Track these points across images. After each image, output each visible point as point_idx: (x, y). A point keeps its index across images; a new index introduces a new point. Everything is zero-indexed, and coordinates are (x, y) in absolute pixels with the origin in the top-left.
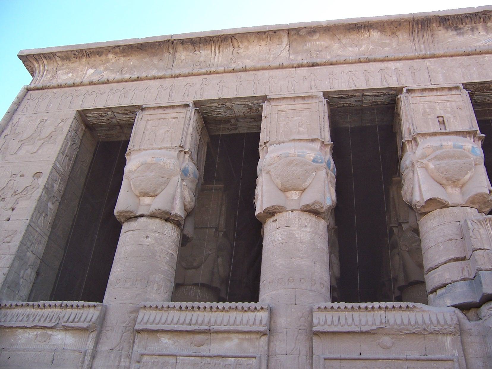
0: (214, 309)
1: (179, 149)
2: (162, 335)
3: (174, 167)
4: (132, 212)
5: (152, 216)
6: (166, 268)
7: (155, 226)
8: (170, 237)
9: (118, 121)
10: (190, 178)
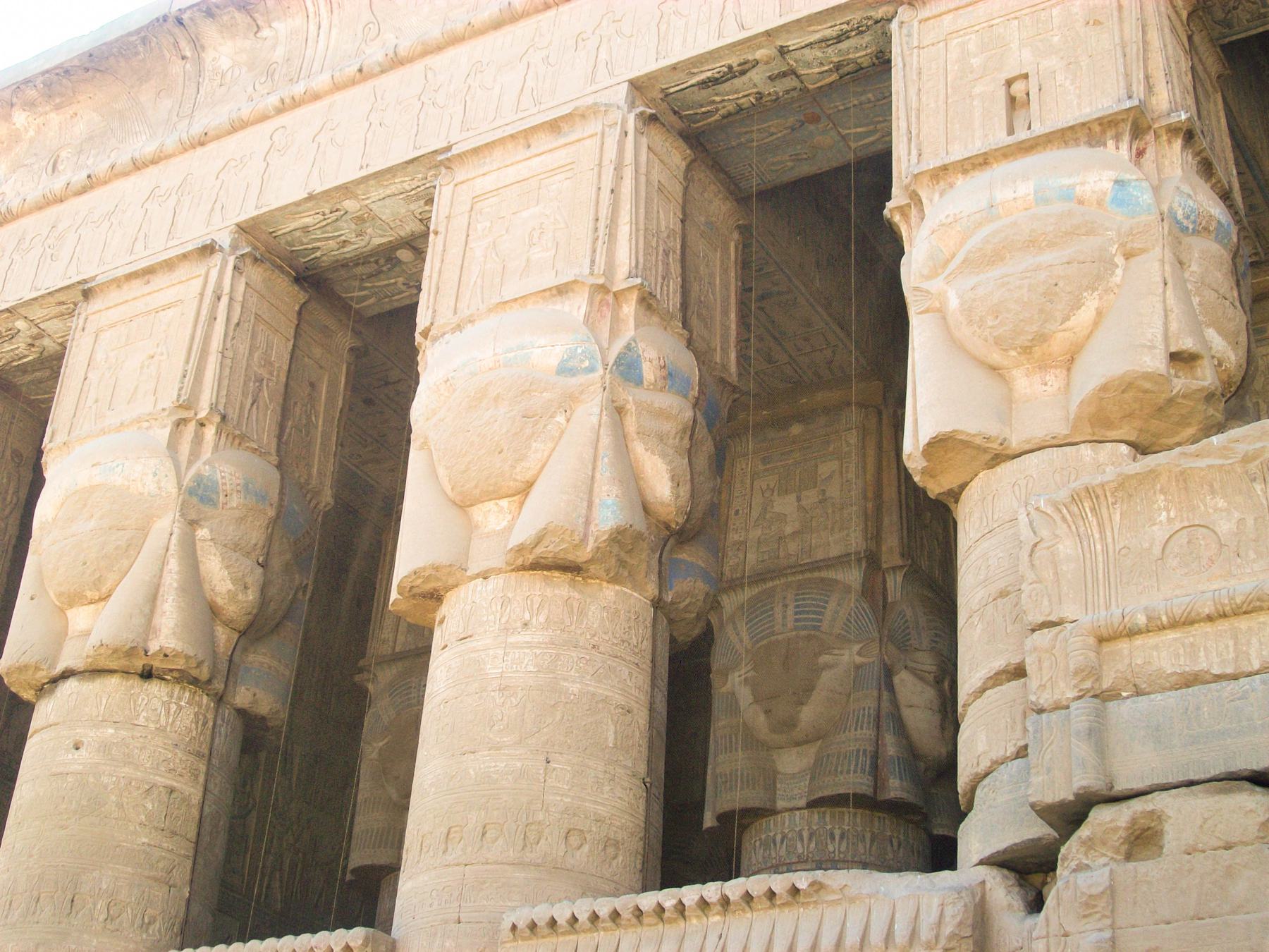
1: (175, 418)
3: (159, 482)
5: (96, 672)
6: (145, 840)
7: (104, 701)
8: (161, 730)
10: (233, 508)
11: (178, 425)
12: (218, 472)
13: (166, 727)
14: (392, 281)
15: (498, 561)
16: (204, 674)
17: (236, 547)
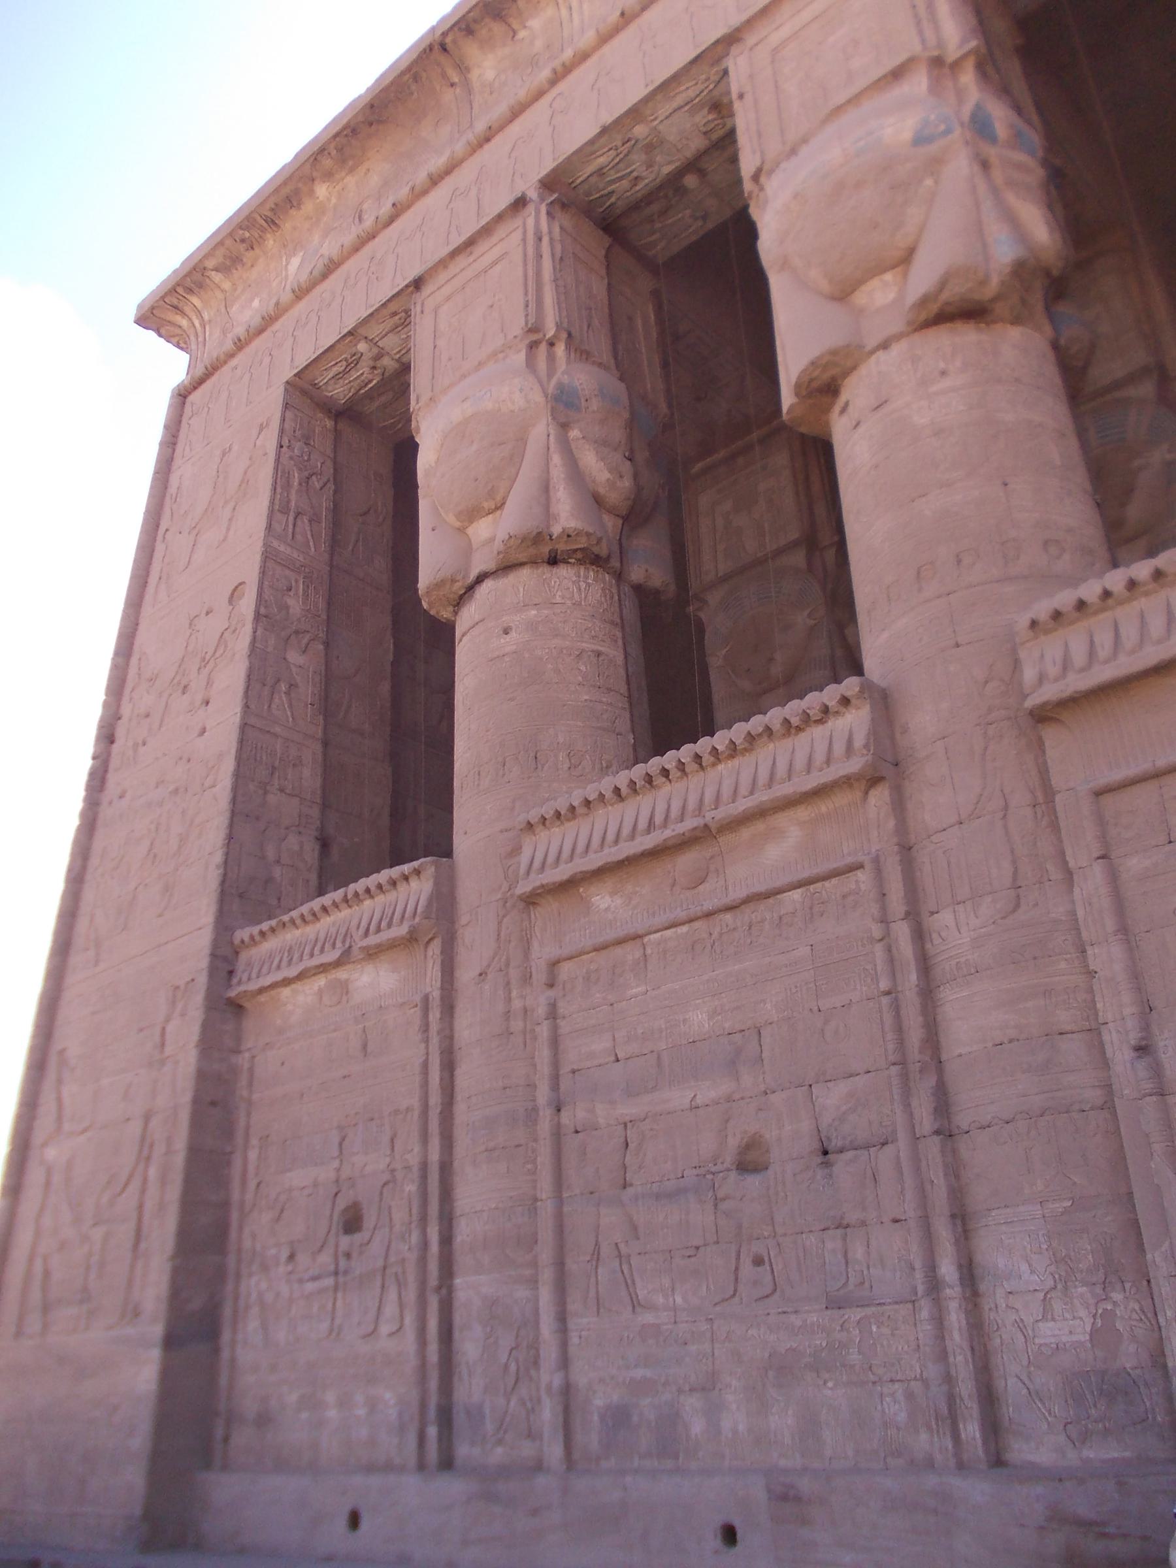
0: (707, 759)
1: (527, 342)
2: (593, 889)
4: (453, 581)
5: (506, 568)
7: (521, 590)
9: (398, 361)
10: (594, 412)
11: (531, 348)
12: (576, 381)
13: (581, 602)
14: (680, 215)
15: (897, 325)
16: (604, 553)
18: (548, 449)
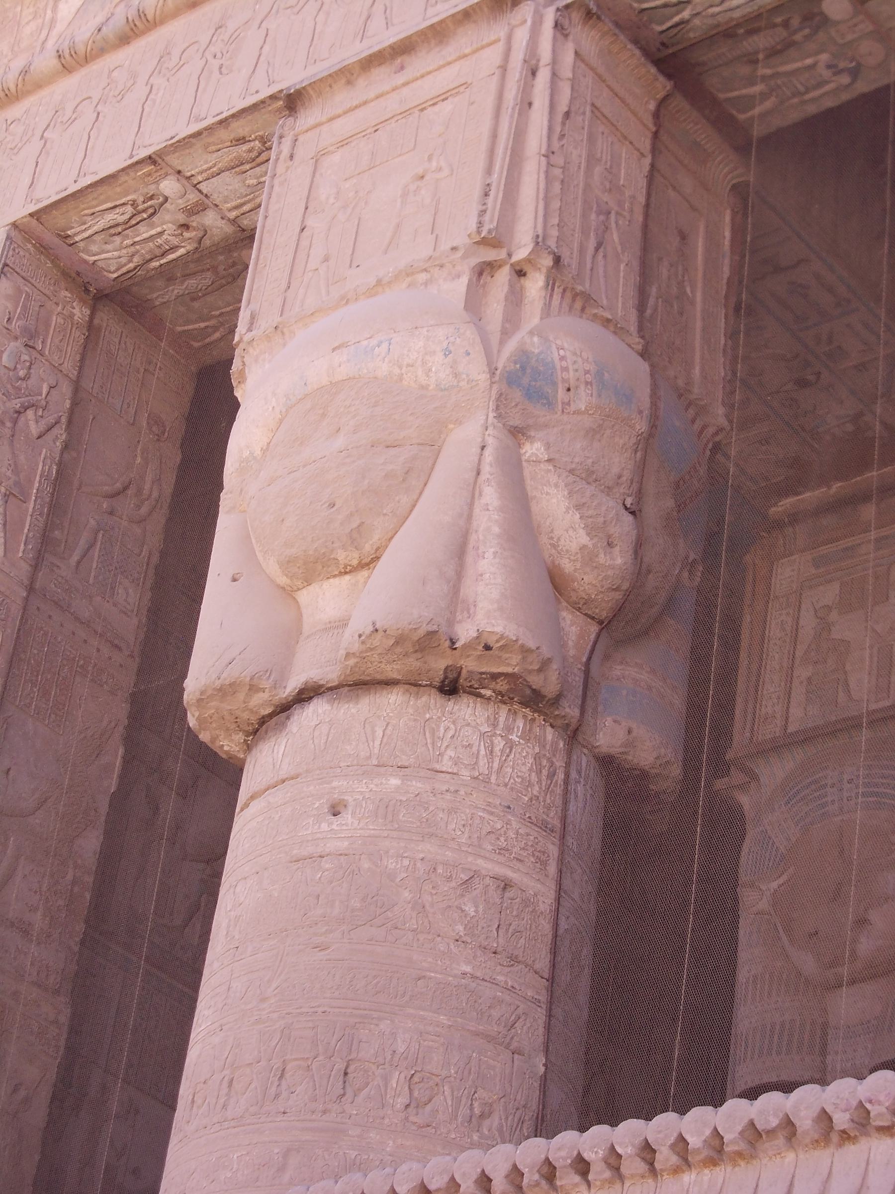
1: (474, 261)
4: (253, 688)
6: (468, 969)
7: (379, 733)
8: (482, 780)
9: (234, 222)
10: (578, 412)
11: (480, 274)
13: (488, 776)
16: (550, 684)
17: (589, 476)
18: (478, 474)
